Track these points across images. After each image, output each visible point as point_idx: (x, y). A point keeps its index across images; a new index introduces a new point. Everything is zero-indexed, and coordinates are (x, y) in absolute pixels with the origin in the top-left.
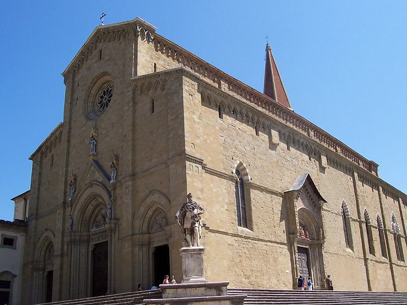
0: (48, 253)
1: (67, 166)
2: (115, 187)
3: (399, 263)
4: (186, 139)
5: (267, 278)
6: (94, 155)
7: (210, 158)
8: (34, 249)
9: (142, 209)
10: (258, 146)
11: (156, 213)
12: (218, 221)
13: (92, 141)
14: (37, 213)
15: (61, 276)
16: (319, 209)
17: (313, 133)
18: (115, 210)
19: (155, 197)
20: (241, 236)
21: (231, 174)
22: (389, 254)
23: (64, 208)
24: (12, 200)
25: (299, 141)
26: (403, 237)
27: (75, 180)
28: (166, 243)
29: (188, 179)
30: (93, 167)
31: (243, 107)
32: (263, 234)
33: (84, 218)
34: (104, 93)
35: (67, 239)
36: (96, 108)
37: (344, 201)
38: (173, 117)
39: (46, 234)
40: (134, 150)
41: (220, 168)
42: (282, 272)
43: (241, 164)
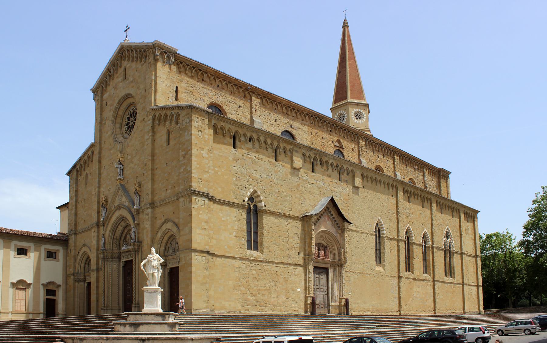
0: (87, 266)
1: (99, 187)
2: (138, 212)
4: (193, 175)
6: (121, 179)
7: (220, 189)
8: (75, 262)
9: (159, 235)
11: (172, 238)
12: (226, 247)
14: (76, 228)
15: (97, 287)
16: (343, 230)
17: (363, 143)
18: (138, 233)
19: (169, 225)
20: (250, 260)
21: (243, 203)
23: (98, 226)
24: (57, 208)
25: (327, 162)
27: (107, 201)
28: (177, 266)
29: (194, 213)
31: (260, 134)
32: (275, 256)
33: (115, 237)
35: (101, 256)
38: (183, 153)
39: (84, 249)
40: (153, 180)
41: (231, 198)
43: (255, 192)
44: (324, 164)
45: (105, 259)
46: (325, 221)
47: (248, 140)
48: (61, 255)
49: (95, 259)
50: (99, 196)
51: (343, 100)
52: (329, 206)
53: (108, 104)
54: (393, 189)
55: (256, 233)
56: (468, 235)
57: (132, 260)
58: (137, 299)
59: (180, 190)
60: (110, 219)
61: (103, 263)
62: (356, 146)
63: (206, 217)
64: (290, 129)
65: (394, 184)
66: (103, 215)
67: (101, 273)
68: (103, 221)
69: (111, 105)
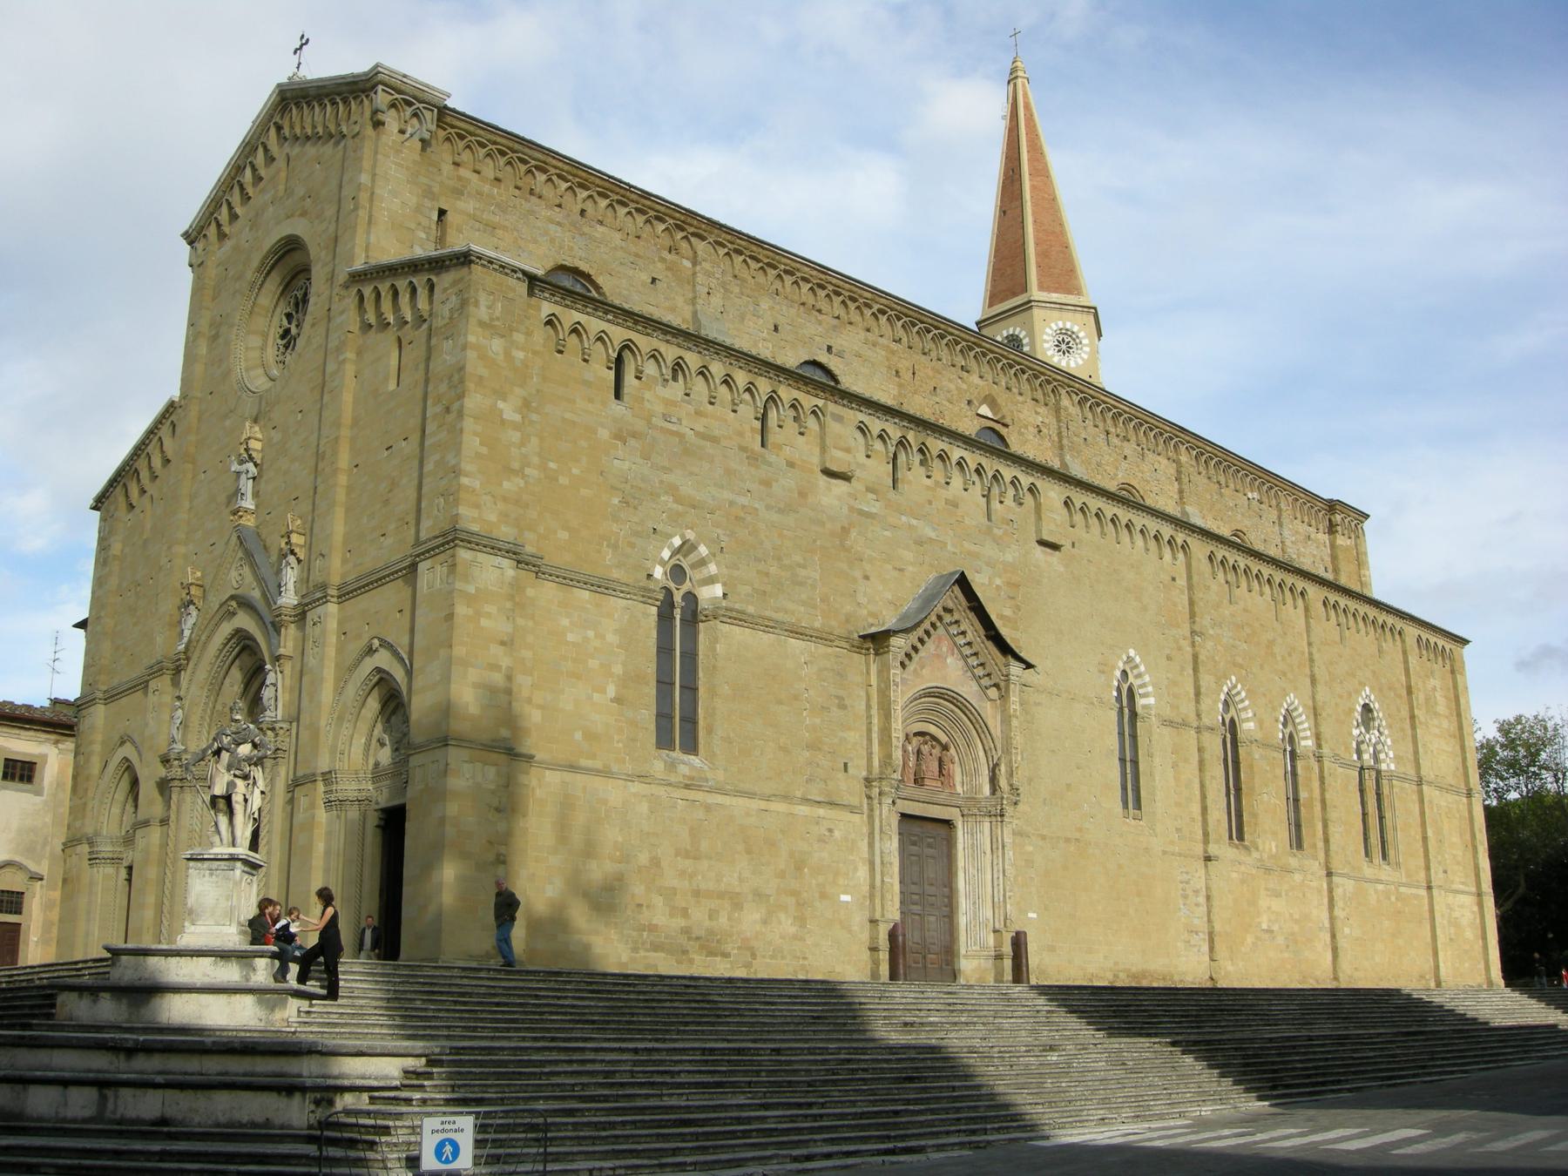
3: (1368, 871)
5: (757, 916)
7: (563, 535)
10: (767, 483)
12: (578, 736)
13: (244, 467)
16: (1002, 687)
17: (1075, 411)
21: (644, 583)
22: (1326, 841)
25: (943, 457)
26: (1403, 779)
29: (461, 610)
33: (219, 707)
34: (297, 305)
36: (271, 353)
37: (1130, 660)
42: (823, 896)
43: (687, 548)
44: (937, 464)
46: (938, 656)
47: (668, 373)
51: (1015, 294)
52: (950, 605)
54: (1175, 558)
55: (690, 689)
56: (1436, 722)
62: (1051, 420)
63: (501, 627)
64: (823, 358)
65: (1180, 541)
69: (239, 277)
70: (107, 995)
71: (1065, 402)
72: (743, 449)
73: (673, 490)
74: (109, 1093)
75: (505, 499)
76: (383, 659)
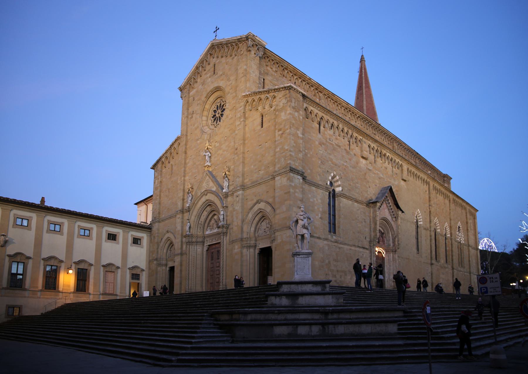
1: (184, 176)
7: (309, 171)
8: (158, 249)
9: (250, 215)
10: (350, 160)
15: (181, 271)
19: (262, 205)
24: (136, 204)
25: (385, 155)
30: (208, 177)
33: (200, 222)
45: (189, 243)
48: (145, 241)
49: (180, 243)
50: (184, 184)
53: (196, 99)
57: (219, 243)
58: (224, 281)
59: (277, 169)
60: (196, 205)
61: (188, 247)
66: (189, 201)
67: (184, 256)
68: (189, 207)
70: (284, 297)
71: (395, 145)
72: (345, 150)
73: (331, 160)
74: (326, 327)
75: (300, 159)
76: (262, 205)
